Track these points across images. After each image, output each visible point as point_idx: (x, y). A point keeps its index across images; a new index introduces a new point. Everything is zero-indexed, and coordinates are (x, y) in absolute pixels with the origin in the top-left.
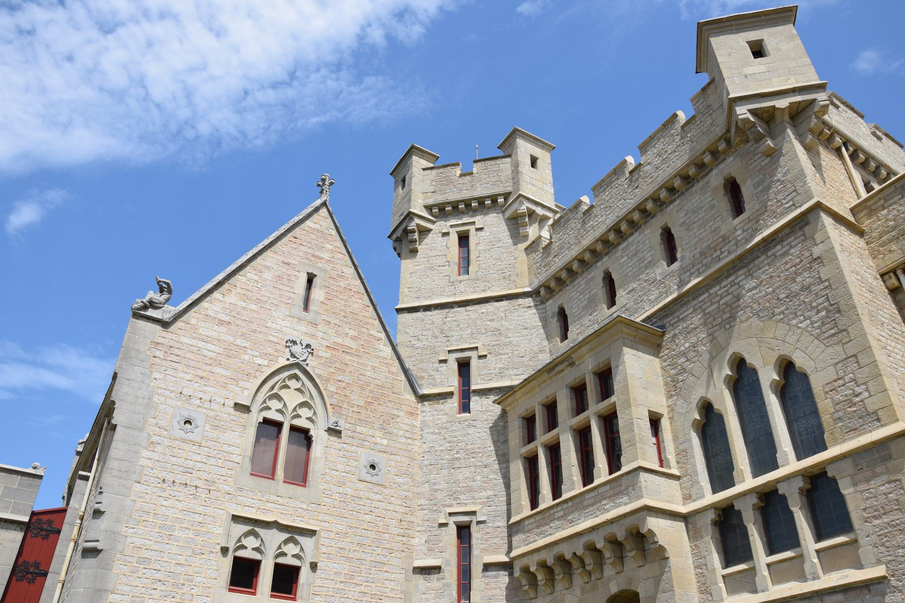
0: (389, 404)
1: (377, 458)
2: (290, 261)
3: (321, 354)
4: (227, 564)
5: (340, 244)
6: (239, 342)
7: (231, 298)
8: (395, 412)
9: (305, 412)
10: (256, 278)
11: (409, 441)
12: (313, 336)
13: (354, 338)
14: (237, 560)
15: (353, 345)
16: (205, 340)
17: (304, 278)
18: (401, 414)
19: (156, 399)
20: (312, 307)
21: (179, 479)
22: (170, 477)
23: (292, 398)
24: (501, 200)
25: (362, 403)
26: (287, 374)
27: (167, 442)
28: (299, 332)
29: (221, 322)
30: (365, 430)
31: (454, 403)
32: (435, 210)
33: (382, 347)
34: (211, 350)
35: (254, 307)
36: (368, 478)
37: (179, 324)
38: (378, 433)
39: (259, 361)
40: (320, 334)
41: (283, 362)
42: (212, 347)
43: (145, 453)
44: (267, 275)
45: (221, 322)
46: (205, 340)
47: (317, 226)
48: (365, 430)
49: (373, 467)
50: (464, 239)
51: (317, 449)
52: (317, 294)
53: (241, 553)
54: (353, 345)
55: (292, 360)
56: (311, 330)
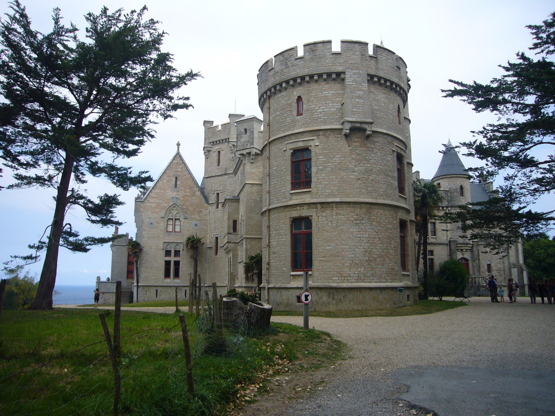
2: (170, 175)
3: (182, 199)
4: (164, 251)
5: (183, 165)
6: (160, 201)
7: (156, 191)
9: (178, 215)
10: (162, 183)
12: (178, 195)
13: (189, 192)
14: (166, 251)
15: (189, 194)
16: (152, 203)
17: (174, 179)
19: (144, 220)
21: (151, 236)
22: (149, 236)
23: (175, 212)
24: (227, 140)
25: (192, 209)
26: (172, 206)
27: (148, 229)
28: (174, 194)
29: (155, 198)
31: (215, 205)
32: (212, 143)
34: (154, 205)
35: (162, 191)
36: (195, 228)
37: (146, 201)
39: (165, 205)
41: (171, 204)
42: (153, 204)
43: (144, 232)
44: (165, 181)
45: (155, 198)
46: (152, 203)
49: (196, 225)
50: (219, 152)
52: (178, 183)
53: (167, 249)
54: (189, 194)
55: (174, 203)
56: (178, 193)
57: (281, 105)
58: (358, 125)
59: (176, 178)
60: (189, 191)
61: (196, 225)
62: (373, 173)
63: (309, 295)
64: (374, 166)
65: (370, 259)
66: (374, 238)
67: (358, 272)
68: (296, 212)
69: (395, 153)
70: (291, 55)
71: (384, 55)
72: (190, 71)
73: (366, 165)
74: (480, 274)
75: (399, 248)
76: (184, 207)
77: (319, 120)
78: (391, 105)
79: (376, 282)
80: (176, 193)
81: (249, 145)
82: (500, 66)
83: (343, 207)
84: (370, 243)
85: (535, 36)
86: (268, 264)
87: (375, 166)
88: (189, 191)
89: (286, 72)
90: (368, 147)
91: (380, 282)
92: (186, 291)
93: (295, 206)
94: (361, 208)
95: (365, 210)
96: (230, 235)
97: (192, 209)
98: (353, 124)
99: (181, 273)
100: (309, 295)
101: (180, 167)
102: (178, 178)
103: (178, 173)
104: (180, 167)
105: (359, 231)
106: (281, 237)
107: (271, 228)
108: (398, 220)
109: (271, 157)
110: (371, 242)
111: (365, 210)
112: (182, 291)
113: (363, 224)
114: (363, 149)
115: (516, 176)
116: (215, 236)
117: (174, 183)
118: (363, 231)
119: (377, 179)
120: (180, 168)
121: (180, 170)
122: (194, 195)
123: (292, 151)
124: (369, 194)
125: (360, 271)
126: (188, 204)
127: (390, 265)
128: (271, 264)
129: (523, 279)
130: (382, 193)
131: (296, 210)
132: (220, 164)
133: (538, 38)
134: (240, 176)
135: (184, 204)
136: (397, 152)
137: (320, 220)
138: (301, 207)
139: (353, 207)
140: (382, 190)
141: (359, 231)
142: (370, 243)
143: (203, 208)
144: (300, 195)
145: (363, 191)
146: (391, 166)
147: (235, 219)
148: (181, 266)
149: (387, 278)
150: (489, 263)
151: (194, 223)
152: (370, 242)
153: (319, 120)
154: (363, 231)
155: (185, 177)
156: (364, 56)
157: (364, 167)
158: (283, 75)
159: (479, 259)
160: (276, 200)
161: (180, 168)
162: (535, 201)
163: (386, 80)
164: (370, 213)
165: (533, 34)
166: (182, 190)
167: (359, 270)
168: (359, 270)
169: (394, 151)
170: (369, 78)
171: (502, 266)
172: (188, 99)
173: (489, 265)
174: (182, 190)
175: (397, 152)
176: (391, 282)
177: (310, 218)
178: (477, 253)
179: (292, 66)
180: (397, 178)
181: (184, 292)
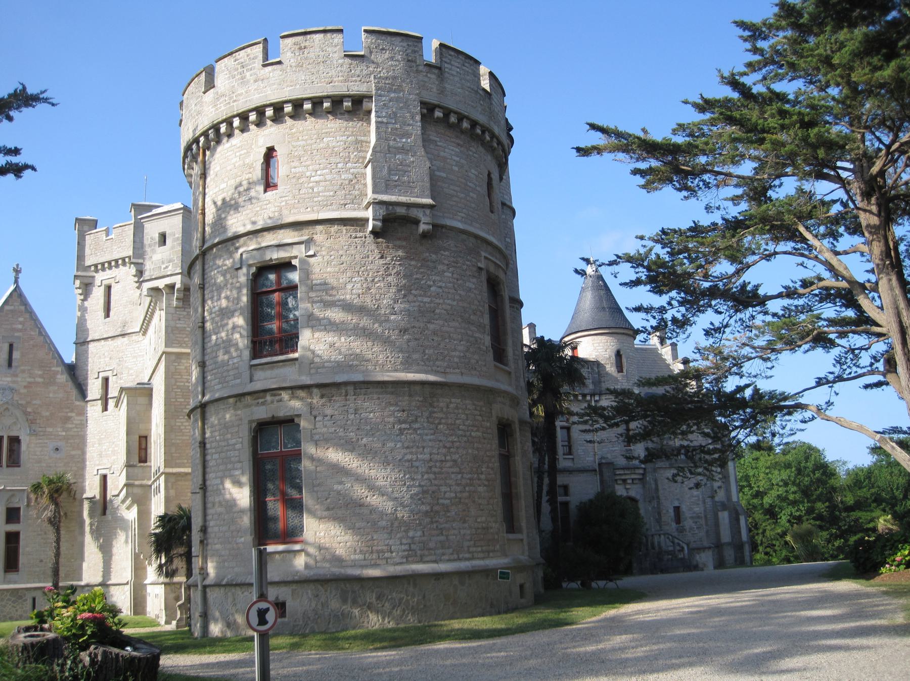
0: (65, 410)
1: (59, 444)
5: (27, 316)
8: (70, 414)
11: (79, 430)
12: (14, 382)
13: (40, 376)
15: (40, 380)
17: (6, 347)
18: (73, 414)
20: (14, 364)
25: (48, 414)
30: (51, 430)
33: (59, 376)
38: (59, 429)
40: (19, 379)
47: (12, 308)
48: (51, 430)
49: (57, 449)
51: (24, 447)
52: (16, 355)
54: (40, 380)
56: (15, 379)
57: (229, 168)
58: (401, 211)
59: (11, 346)
60: (40, 373)
61: (57, 449)
62: (437, 316)
63: (267, 610)
64: (437, 301)
65: (436, 508)
66: (442, 461)
67: (409, 541)
68: (263, 408)
69: (484, 273)
70: (252, 56)
71: (456, 64)
72: (21, 87)
73: (420, 299)
74: (660, 527)
75: (498, 481)
76: (29, 410)
77: (316, 199)
78: (473, 171)
79: (449, 560)
80: (9, 379)
81: (170, 268)
82: (686, 102)
83: (371, 393)
84: (435, 473)
85: (748, 45)
86: (204, 530)
87: (441, 301)
88: (40, 373)
89: (241, 94)
90: (424, 259)
91: (459, 559)
92: (34, 599)
93: (262, 394)
94: (410, 396)
95: (421, 399)
96: (131, 469)
97: (48, 414)
98: (391, 207)
99: (22, 560)
100: (267, 610)
101: (21, 319)
102: (15, 345)
103: (16, 334)
104: (21, 319)
105: (408, 448)
106: (229, 466)
107: (208, 446)
108: (494, 418)
109: (207, 285)
110: (436, 470)
111: (421, 399)
112: (26, 600)
113: (415, 430)
114: (413, 263)
115: (727, 326)
116: (100, 472)
117: (5, 355)
118: (418, 447)
119: (445, 329)
120: (21, 323)
121: (20, 327)
122: (50, 381)
123: (253, 270)
124: (427, 363)
125: (413, 538)
126: (38, 402)
127: (479, 520)
128: (209, 530)
129: (740, 532)
130: (456, 360)
131: (263, 404)
132: (111, 313)
133: (755, 50)
134: (153, 337)
135: (28, 403)
136: (488, 272)
137: (318, 425)
138: (275, 395)
139: (392, 393)
140: (457, 353)
141: (408, 448)
142: (435, 473)
143: (72, 411)
144: (272, 368)
145: (415, 356)
146: (476, 302)
147: (143, 433)
148: (22, 543)
149: (474, 549)
150: (677, 504)
151: (52, 445)
152: (434, 469)
153: (316, 199)
154: (418, 447)
155: (32, 342)
156: (413, 64)
157: (417, 304)
158: (235, 101)
159: (658, 498)
160: (219, 383)
161: (21, 323)
162: (769, 373)
163: (461, 117)
164: (431, 405)
165: (745, 40)
166: (23, 371)
167: (411, 534)
168: (411, 534)
169: (480, 269)
170: (425, 111)
171: (702, 509)
172: (16, 151)
173: (677, 509)
174: (23, 371)
175: (488, 272)
176: (483, 558)
177: (296, 420)
178: (653, 486)
179: (256, 81)
180: (488, 328)
181: (30, 602)
